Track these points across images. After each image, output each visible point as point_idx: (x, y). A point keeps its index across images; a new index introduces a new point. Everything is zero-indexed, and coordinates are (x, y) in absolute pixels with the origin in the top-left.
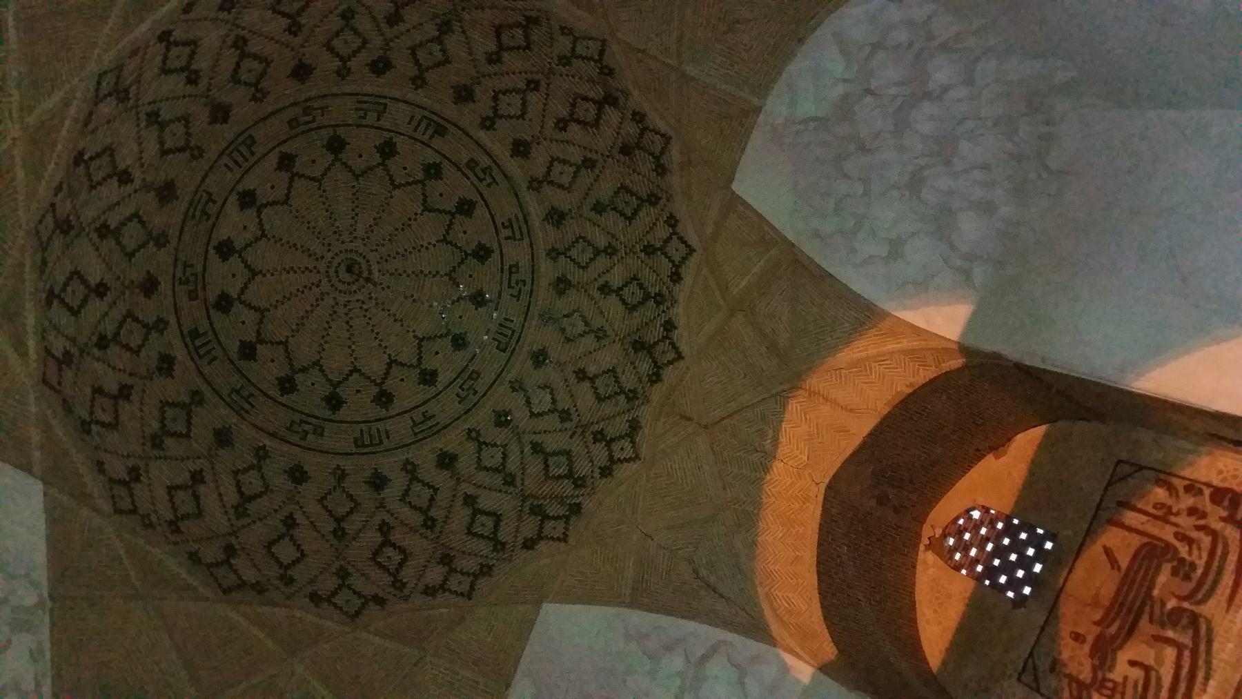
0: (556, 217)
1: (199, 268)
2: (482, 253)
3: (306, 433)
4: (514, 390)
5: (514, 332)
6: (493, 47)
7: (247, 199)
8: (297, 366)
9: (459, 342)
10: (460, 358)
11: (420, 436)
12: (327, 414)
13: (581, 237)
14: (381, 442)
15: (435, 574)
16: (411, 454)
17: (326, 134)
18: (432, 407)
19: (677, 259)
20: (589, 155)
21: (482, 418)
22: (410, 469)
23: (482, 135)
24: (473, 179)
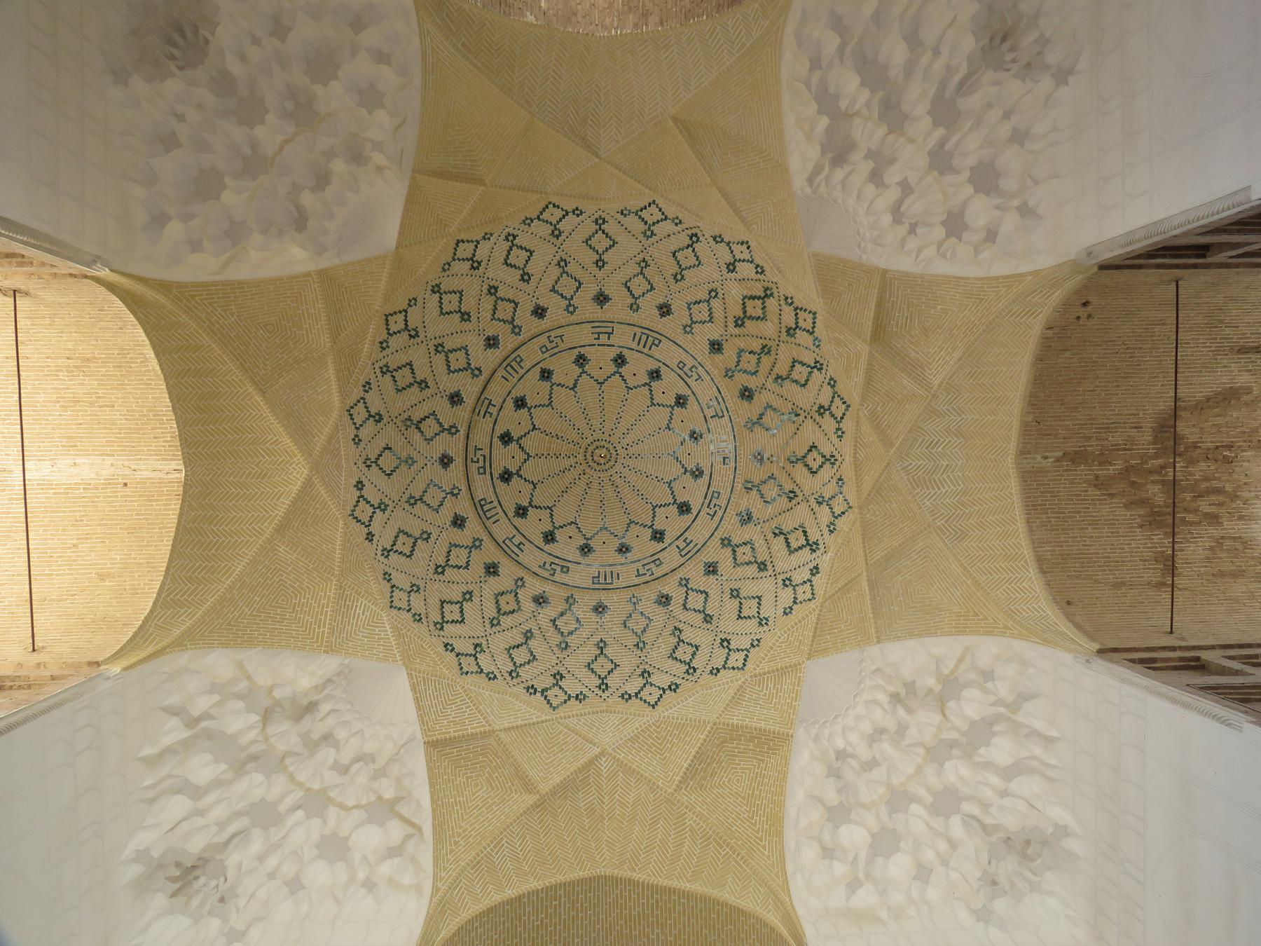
1: (562, 346)
2: (658, 536)
6: (800, 454)
7: (620, 361)
8: (522, 442)
9: (586, 549)
10: (574, 555)
12: (496, 475)
15: (401, 580)
16: (488, 544)
17: (684, 391)
18: (527, 547)
19: (730, 664)
21: (534, 586)
22: (476, 544)
23: (738, 486)
24: (707, 501)
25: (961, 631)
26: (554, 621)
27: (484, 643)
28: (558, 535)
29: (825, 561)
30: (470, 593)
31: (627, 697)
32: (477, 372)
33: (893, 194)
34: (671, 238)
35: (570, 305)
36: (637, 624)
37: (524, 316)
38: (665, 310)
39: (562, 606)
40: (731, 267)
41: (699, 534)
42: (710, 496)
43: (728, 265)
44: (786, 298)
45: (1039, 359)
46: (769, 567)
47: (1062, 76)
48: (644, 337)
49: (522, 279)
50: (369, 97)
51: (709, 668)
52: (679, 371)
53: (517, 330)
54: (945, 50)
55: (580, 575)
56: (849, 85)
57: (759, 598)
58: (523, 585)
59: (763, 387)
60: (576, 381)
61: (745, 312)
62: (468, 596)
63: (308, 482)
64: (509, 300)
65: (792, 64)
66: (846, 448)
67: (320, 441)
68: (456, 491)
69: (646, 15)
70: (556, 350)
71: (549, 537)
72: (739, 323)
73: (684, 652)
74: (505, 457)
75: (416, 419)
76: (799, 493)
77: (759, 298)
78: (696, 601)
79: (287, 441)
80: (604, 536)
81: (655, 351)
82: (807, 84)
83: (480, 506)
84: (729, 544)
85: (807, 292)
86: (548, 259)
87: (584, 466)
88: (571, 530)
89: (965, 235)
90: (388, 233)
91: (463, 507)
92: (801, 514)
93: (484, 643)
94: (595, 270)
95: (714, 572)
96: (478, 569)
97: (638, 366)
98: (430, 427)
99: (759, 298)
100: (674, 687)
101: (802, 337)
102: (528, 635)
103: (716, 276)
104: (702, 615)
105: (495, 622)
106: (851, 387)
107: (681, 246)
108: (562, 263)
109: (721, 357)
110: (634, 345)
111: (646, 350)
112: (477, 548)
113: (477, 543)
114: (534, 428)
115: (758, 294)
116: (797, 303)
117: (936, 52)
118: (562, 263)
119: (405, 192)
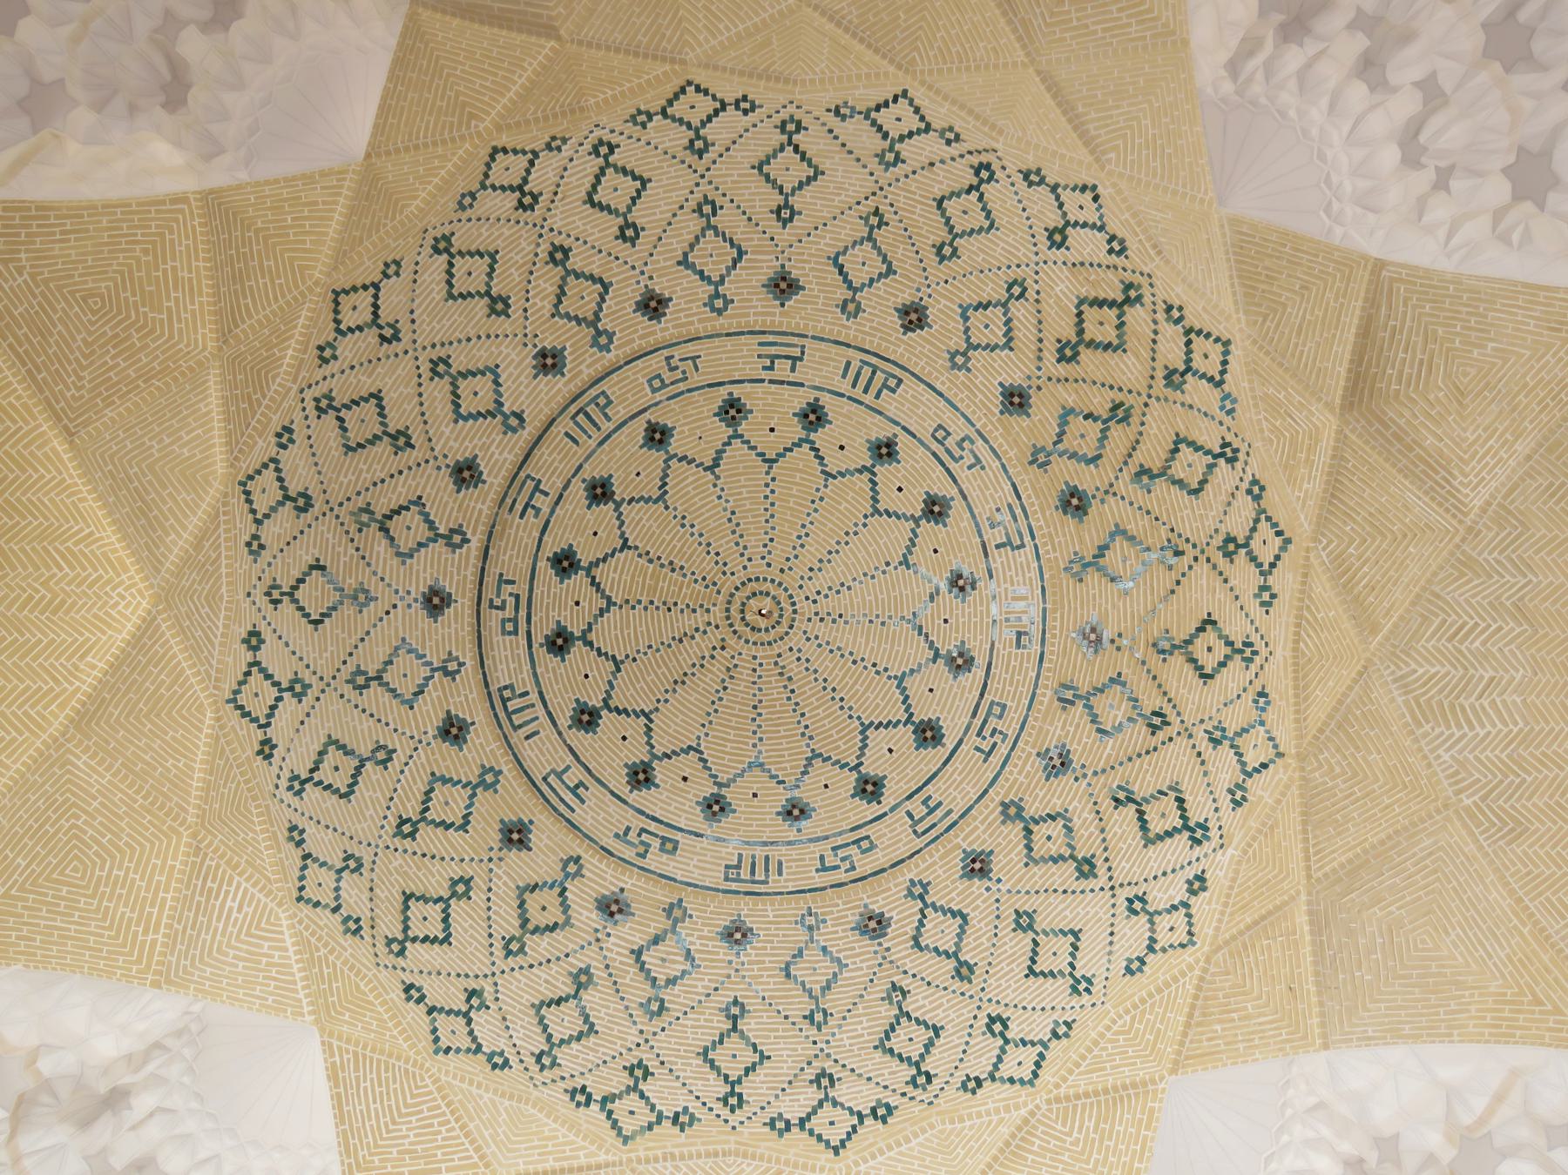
0: (977, 866)
1: (696, 379)
3: (502, 608)
4: (669, 911)
5: (765, 882)
7: (813, 416)
8: (597, 572)
9: (715, 806)
10: (692, 817)
11: (544, 788)
12: (538, 639)
13: (964, 917)
14: (516, 728)
15: (321, 843)
18: (593, 793)
19: (1006, 1070)
20: (1099, 862)
21: (602, 877)
22: (487, 780)
23: (1046, 696)
24: (978, 722)
25: (1503, 1033)
26: (638, 953)
27: (489, 989)
28: (660, 771)
29: (1219, 865)
30: (467, 882)
31: (780, 1126)
32: (514, 422)
33: (1405, 105)
34: (934, 169)
35: (717, 295)
36: (814, 970)
37: (620, 312)
39: (659, 923)
40: (1058, 237)
41: (954, 790)
42: (985, 712)
43: (1051, 233)
44: (1169, 309)
46: (1101, 870)
48: (867, 371)
49: (622, 236)
51: (960, 1077)
52: (935, 446)
53: (603, 340)
55: (700, 861)
57: (1076, 934)
58: (578, 874)
59: (1110, 491)
60: (720, 452)
61: (1081, 332)
62: (461, 888)
63: (148, 627)
64: (591, 278)
66: (1278, 627)
67: (178, 543)
68: (452, 666)
70: (682, 386)
71: (641, 776)
72: (1067, 353)
73: (908, 1040)
74: (561, 603)
75: (381, 509)
76: (1172, 717)
77: (1112, 304)
78: (940, 932)
79: (110, 537)
80: (756, 781)
81: (888, 402)
83: (500, 701)
84: (1019, 816)
85: (1213, 298)
86: (677, 197)
87: (724, 632)
88: (688, 764)
89: (1553, 198)
90: (354, 126)
91: (466, 700)
92: (1176, 762)
93: (489, 989)
94: (774, 227)
95: (984, 872)
96: (486, 832)
97: (850, 430)
98: (409, 528)
99: (1112, 304)
100: (882, 1112)
102: (582, 980)
103: (1024, 253)
104: (952, 963)
105: (514, 946)
106: (1294, 502)
107: (957, 187)
108: (707, 208)
109: (1024, 422)
110: (845, 387)
111: (868, 399)
112: (487, 787)
113: (489, 778)
114: (625, 545)
115: (1111, 295)
116: (1191, 320)
118: (707, 208)
119: (393, 42)
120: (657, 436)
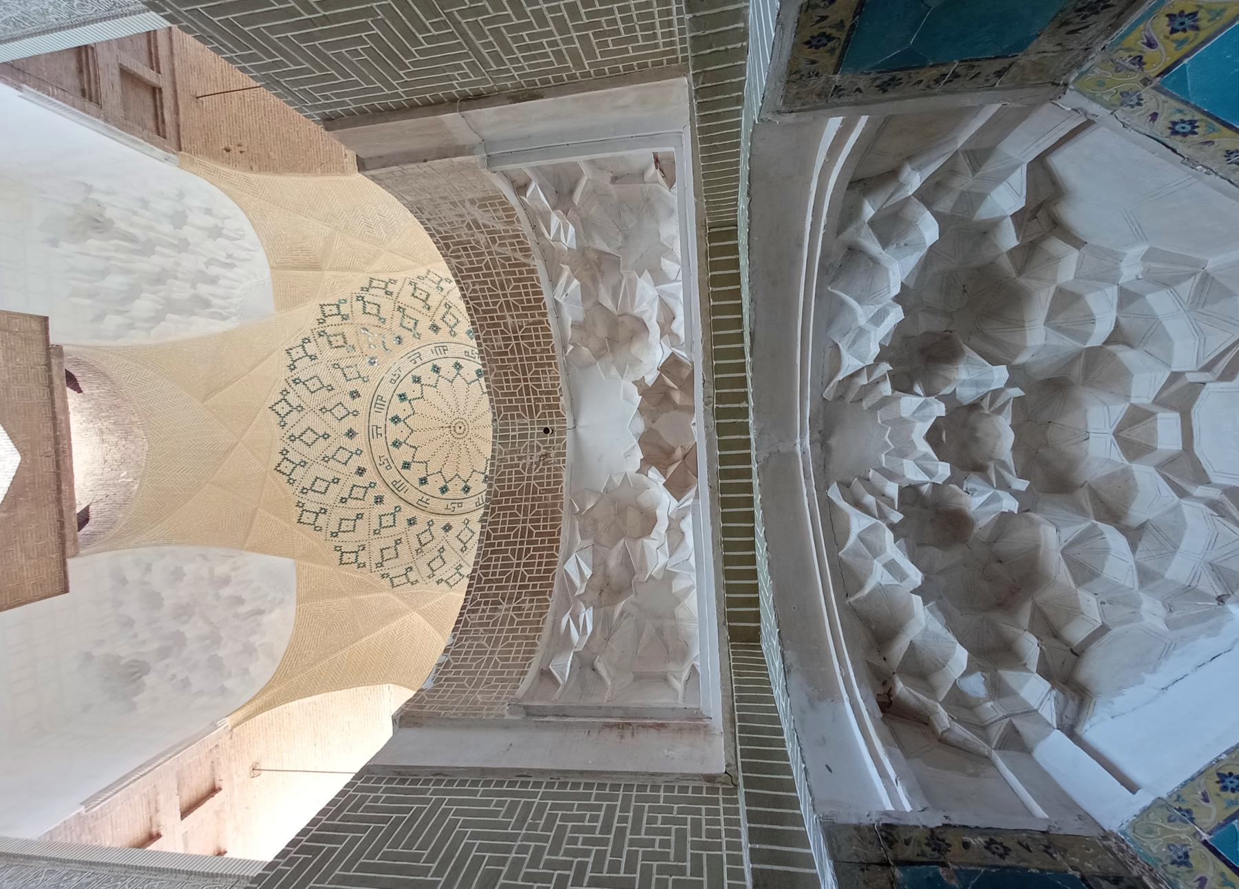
1: (387, 456)
7: (396, 420)
23: (455, 339)
38: (355, 395)
45: (276, 171)
47: (89, 189)
50: (177, 575)
54: (106, 254)
56: (144, 305)
65: (138, 338)
67: (402, 605)
69: (132, 423)
81: (387, 398)
82: (149, 330)
86: (322, 468)
90: (285, 564)
97: (399, 408)
98: (425, 537)
101: (345, 309)
108: (326, 459)
110: (384, 412)
117: (109, 258)
118: (326, 459)
119: (255, 554)
120: (406, 466)
